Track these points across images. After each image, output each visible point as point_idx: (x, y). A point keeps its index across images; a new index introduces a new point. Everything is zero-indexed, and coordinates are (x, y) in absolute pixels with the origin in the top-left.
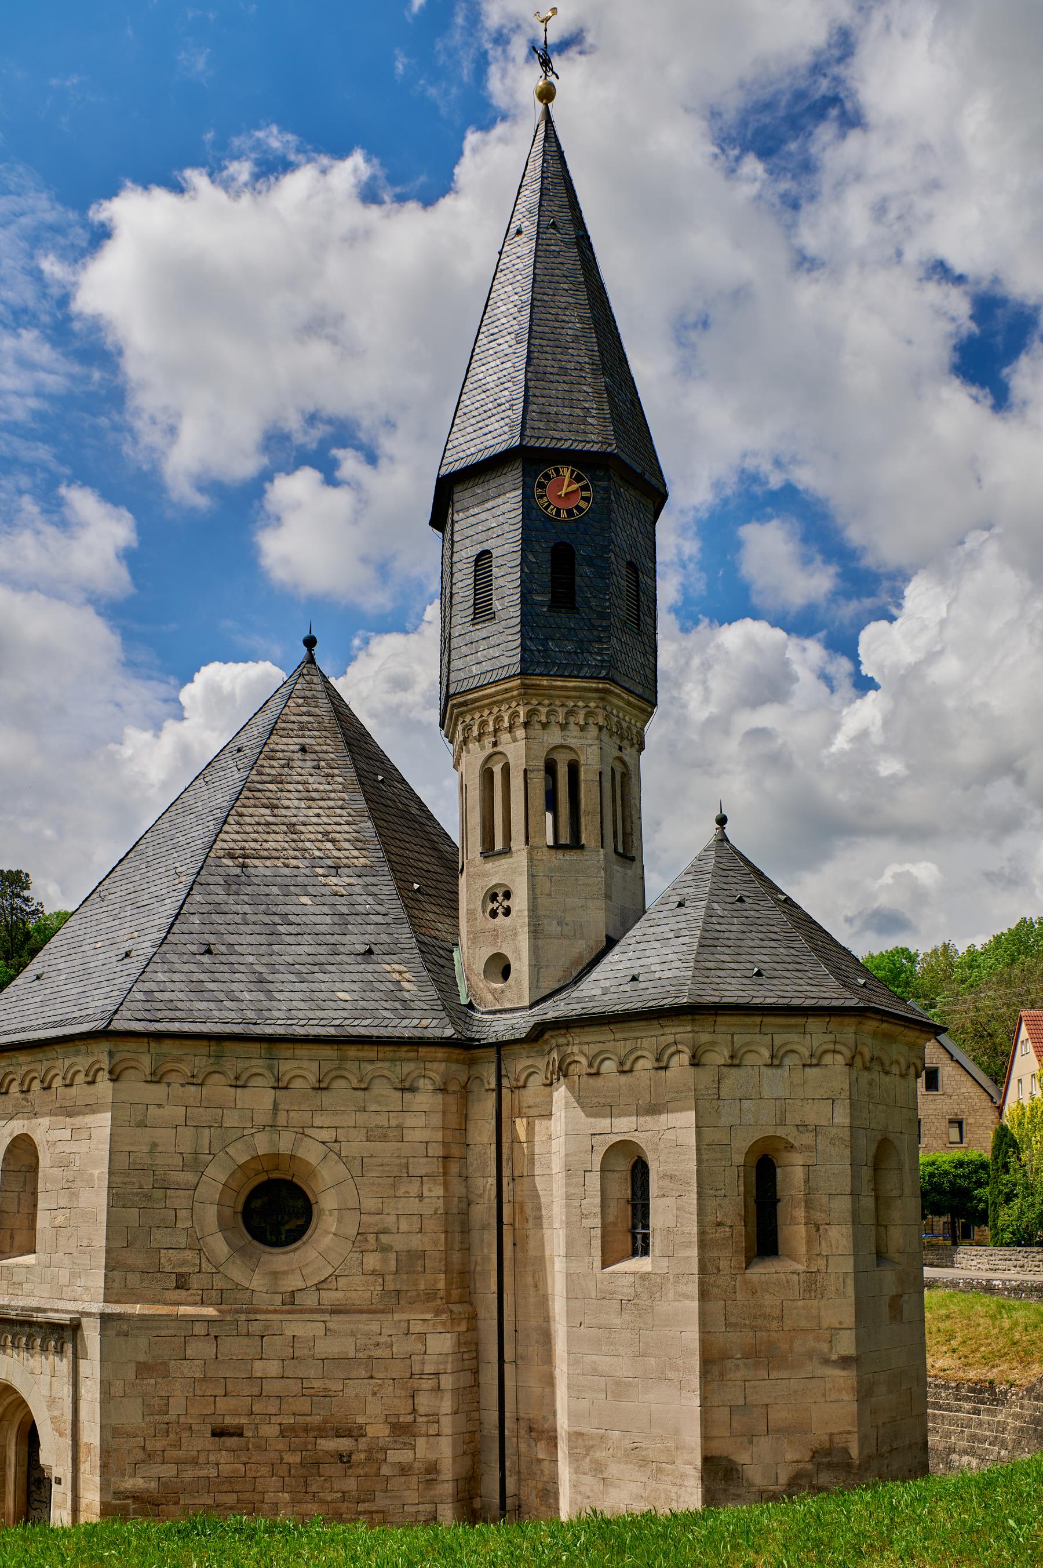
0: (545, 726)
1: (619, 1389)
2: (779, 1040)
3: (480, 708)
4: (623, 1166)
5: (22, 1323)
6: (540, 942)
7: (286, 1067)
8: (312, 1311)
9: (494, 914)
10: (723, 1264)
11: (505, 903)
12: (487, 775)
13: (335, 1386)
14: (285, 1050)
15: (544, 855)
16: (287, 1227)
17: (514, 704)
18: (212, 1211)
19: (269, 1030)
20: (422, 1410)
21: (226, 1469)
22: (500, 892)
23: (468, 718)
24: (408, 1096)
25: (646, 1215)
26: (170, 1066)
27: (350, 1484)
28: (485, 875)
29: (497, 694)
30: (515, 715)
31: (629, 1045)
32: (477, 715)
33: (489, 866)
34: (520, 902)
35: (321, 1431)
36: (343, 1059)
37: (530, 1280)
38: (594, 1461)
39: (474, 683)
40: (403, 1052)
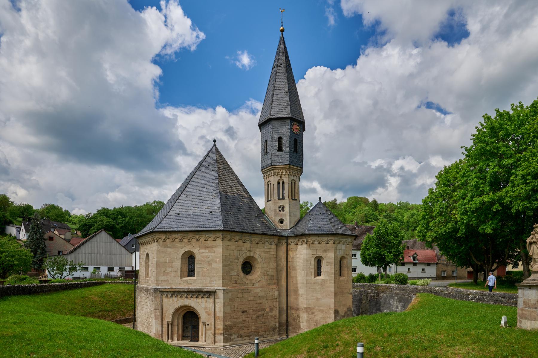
0: (291, 175)
1: (318, 299)
2: (345, 240)
3: (278, 169)
4: (316, 260)
5: (195, 292)
6: (291, 217)
7: (253, 239)
8: (258, 287)
9: (280, 211)
10: (337, 277)
11: (283, 209)
12: (279, 183)
13: (261, 301)
14: (253, 235)
15: (291, 200)
16: (247, 271)
17: (286, 170)
18: (240, 267)
19: (251, 232)
20: (274, 305)
21: (244, 319)
22: (282, 207)
23: (275, 171)
24: (271, 245)
25: (321, 269)
26: (233, 238)
27: (263, 320)
28: (278, 203)
29: (283, 167)
30: (286, 172)
31: (321, 239)
32: (277, 171)
33: (279, 201)
34: (287, 209)
35: (259, 310)
36: (262, 238)
37: (291, 281)
38: (312, 312)
39: (278, 164)
40: (272, 237)
